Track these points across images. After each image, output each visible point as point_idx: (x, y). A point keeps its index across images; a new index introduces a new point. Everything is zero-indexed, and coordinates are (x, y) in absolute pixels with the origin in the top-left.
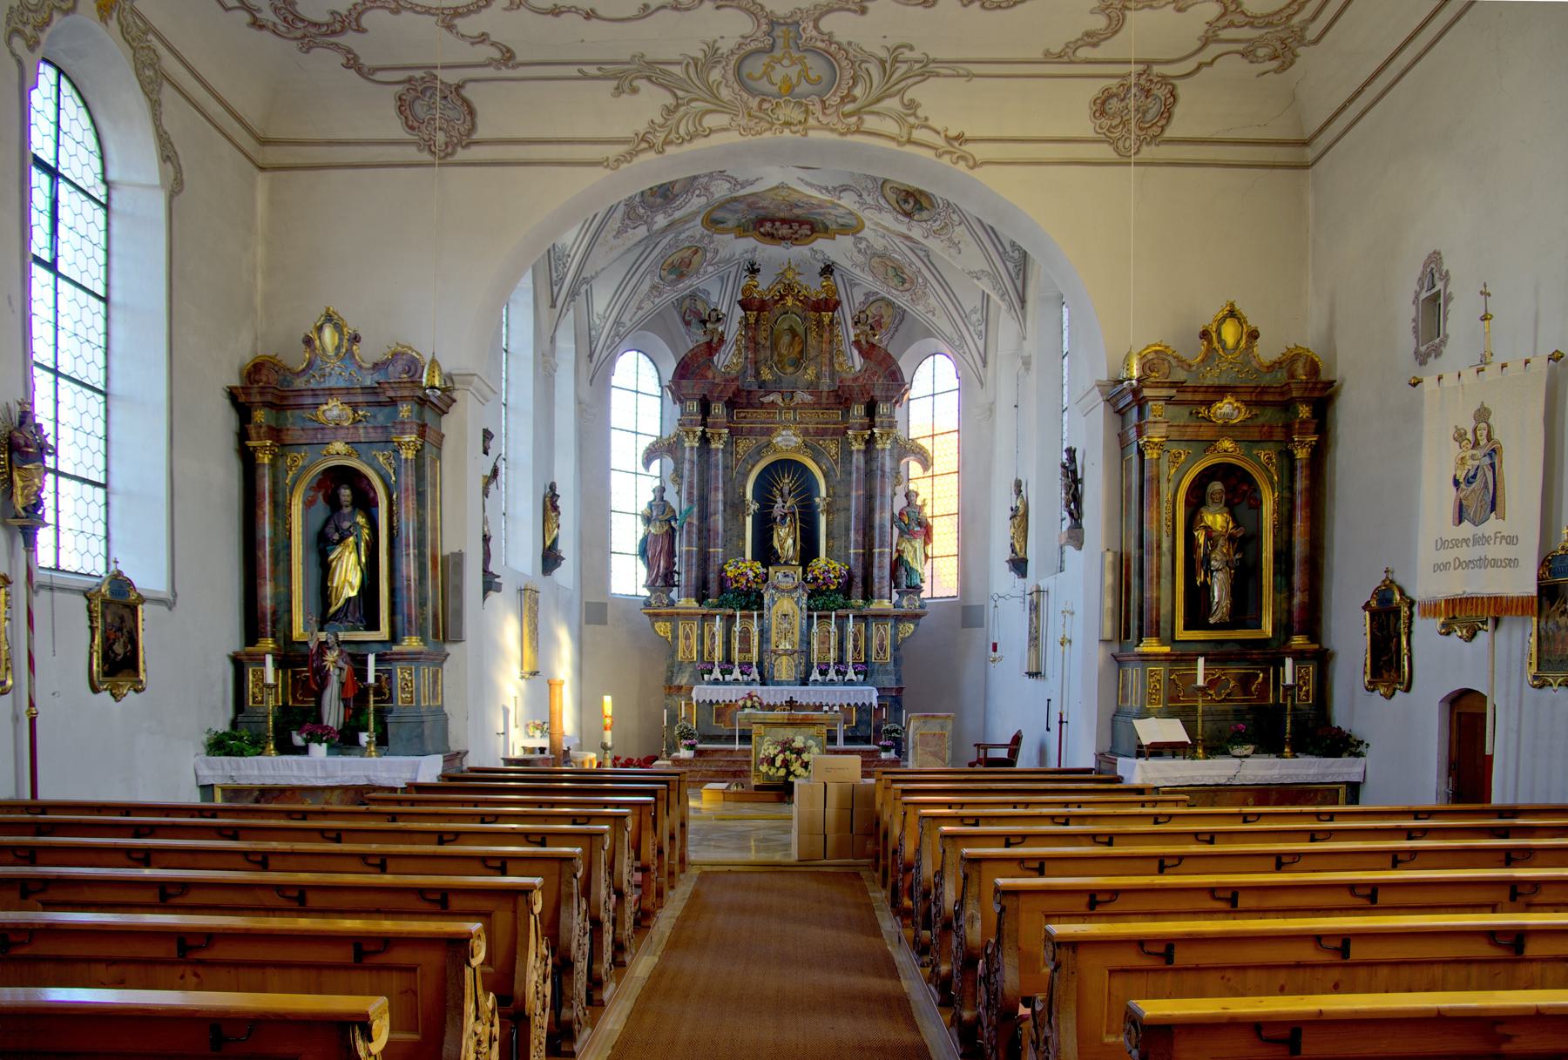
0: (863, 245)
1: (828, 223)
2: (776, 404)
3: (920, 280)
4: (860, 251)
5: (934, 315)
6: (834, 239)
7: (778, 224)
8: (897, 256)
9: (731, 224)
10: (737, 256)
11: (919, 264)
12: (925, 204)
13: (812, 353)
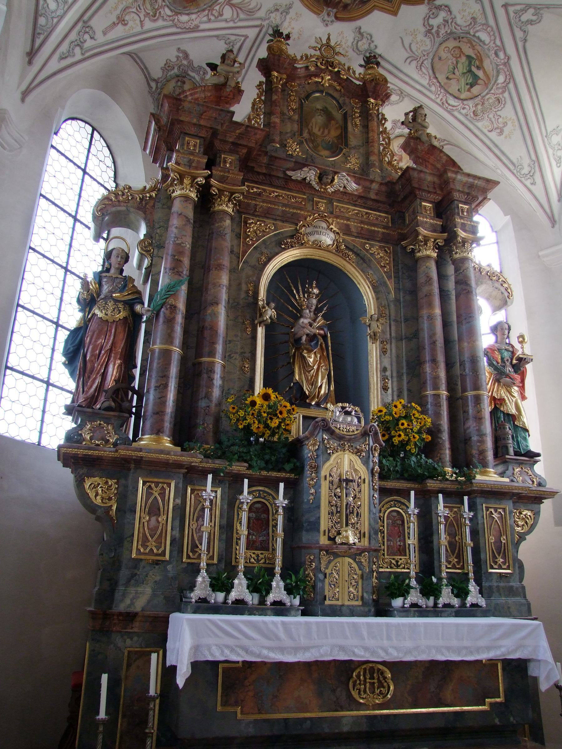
0: (435, 22)
2: (309, 185)
3: (501, 79)
4: (429, 31)
5: (501, 133)
6: (395, 13)
8: (483, 36)
10: (261, 14)
11: (511, 49)
13: (353, 141)
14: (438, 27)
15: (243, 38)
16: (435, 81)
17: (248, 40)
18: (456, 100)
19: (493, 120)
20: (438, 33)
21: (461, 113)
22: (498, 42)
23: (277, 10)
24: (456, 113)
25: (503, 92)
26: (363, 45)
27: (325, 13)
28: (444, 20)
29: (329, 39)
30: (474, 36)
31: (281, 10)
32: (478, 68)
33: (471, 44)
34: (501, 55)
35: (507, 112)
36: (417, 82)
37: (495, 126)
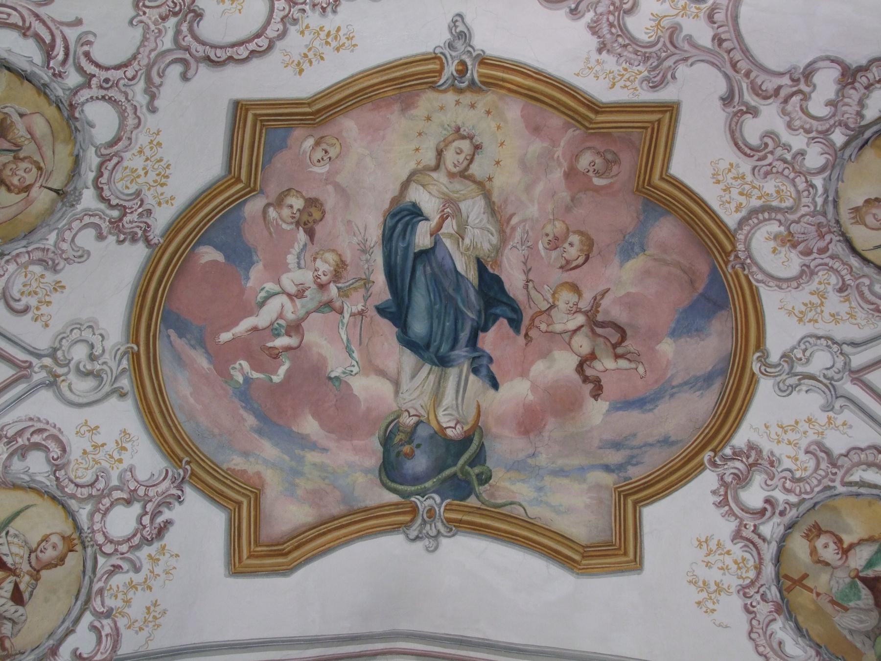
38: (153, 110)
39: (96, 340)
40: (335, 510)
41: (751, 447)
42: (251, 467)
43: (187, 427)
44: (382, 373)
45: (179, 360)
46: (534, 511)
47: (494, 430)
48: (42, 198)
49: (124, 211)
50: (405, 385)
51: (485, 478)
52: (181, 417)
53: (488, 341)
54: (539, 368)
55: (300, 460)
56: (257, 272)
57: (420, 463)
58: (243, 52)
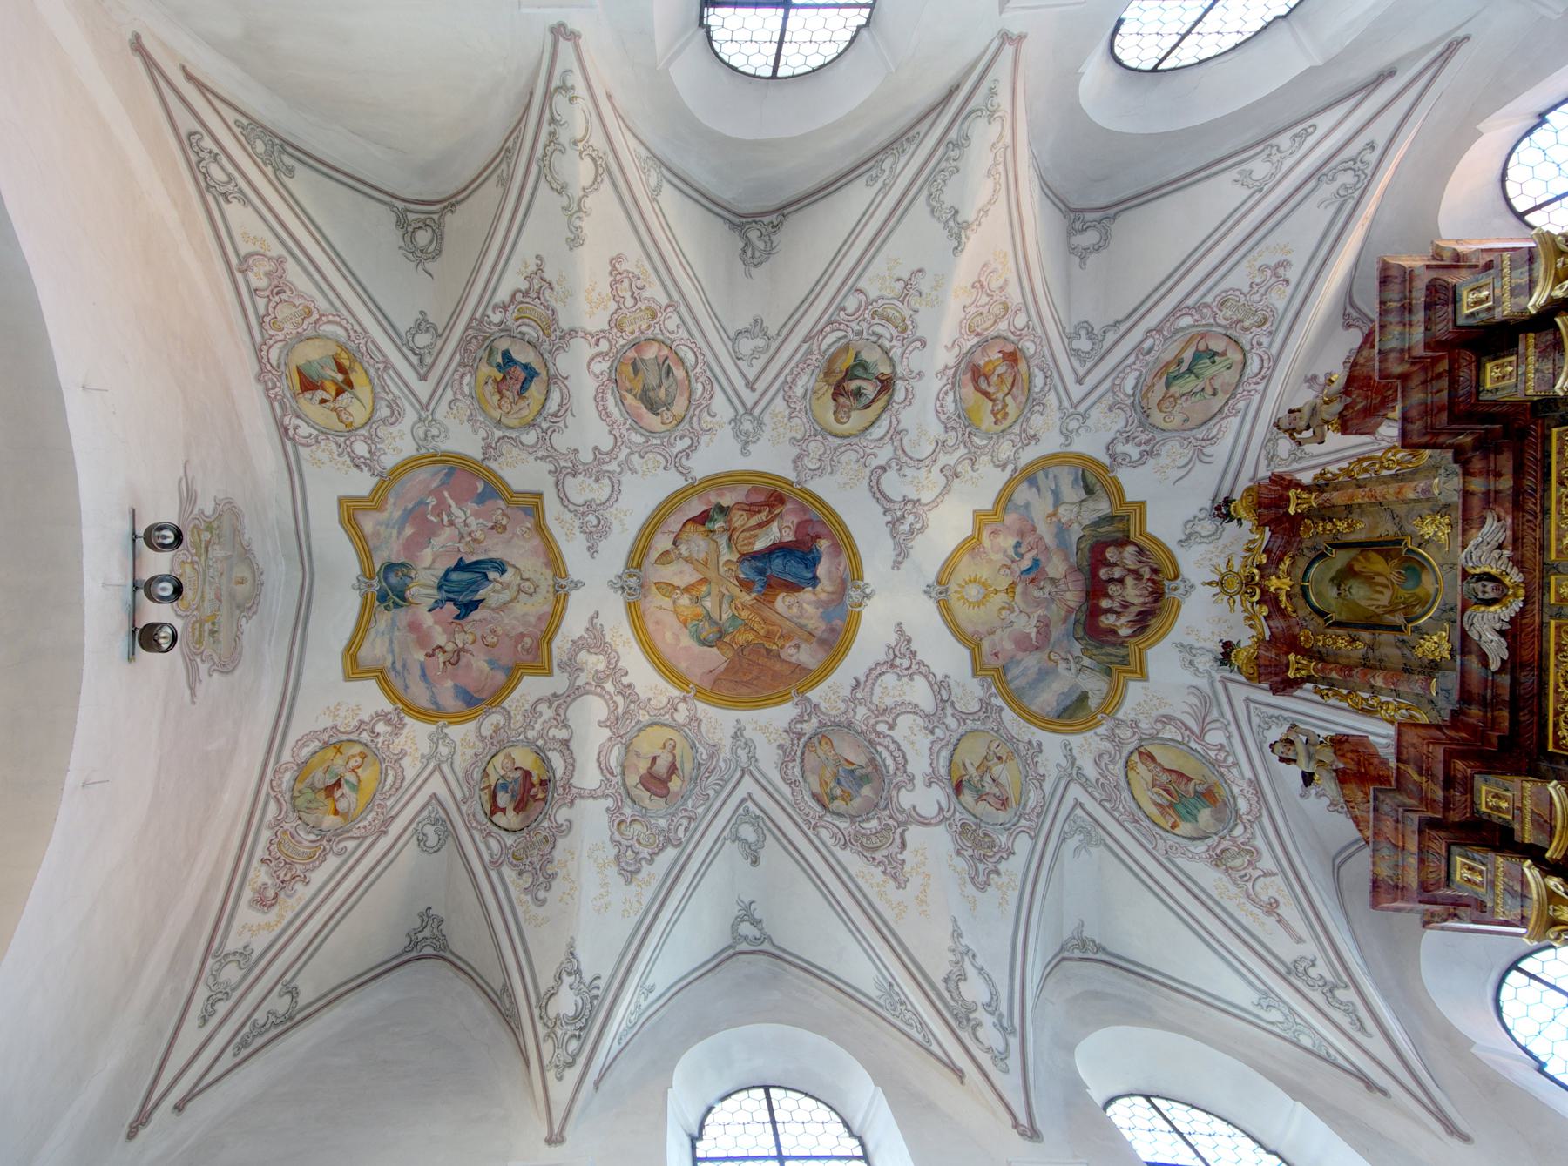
1: (1089, 515)
3: (1186, 321)
4: (1150, 453)
5: (1284, 264)
6: (1142, 505)
7: (1105, 603)
9: (1095, 685)
12: (849, 361)
14: (1139, 445)
15: (1252, 705)
16: (1226, 409)
17: (1253, 697)
18: (1249, 362)
19: (1262, 291)
20: (1148, 442)
21: (1271, 344)
22: (1131, 359)
23: (1191, 663)
24: (1274, 350)
25: (1207, 305)
26: (1207, 527)
27: (1174, 595)
28: (1127, 442)
29: (1210, 584)
30: (1134, 395)
31: (1189, 657)
32: (1180, 363)
33: (1147, 391)
34: (1146, 345)
35: (1239, 279)
36: (1239, 432)
37: (1273, 280)
38: (536, 459)
39: (441, 438)
40: (370, 544)
41: (404, 725)
42: (389, 506)
43: (406, 477)
44: (433, 562)
45: (435, 474)
46: (373, 631)
47: (410, 611)
48: (497, 414)
49: (495, 449)
50: (429, 572)
51: (387, 608)
52: (410, 475)
53: (450, 606)
54: (439, 629)
55: (393, 527)
56: (475, 506)
57: (393, 580)
58: (562, 495)
